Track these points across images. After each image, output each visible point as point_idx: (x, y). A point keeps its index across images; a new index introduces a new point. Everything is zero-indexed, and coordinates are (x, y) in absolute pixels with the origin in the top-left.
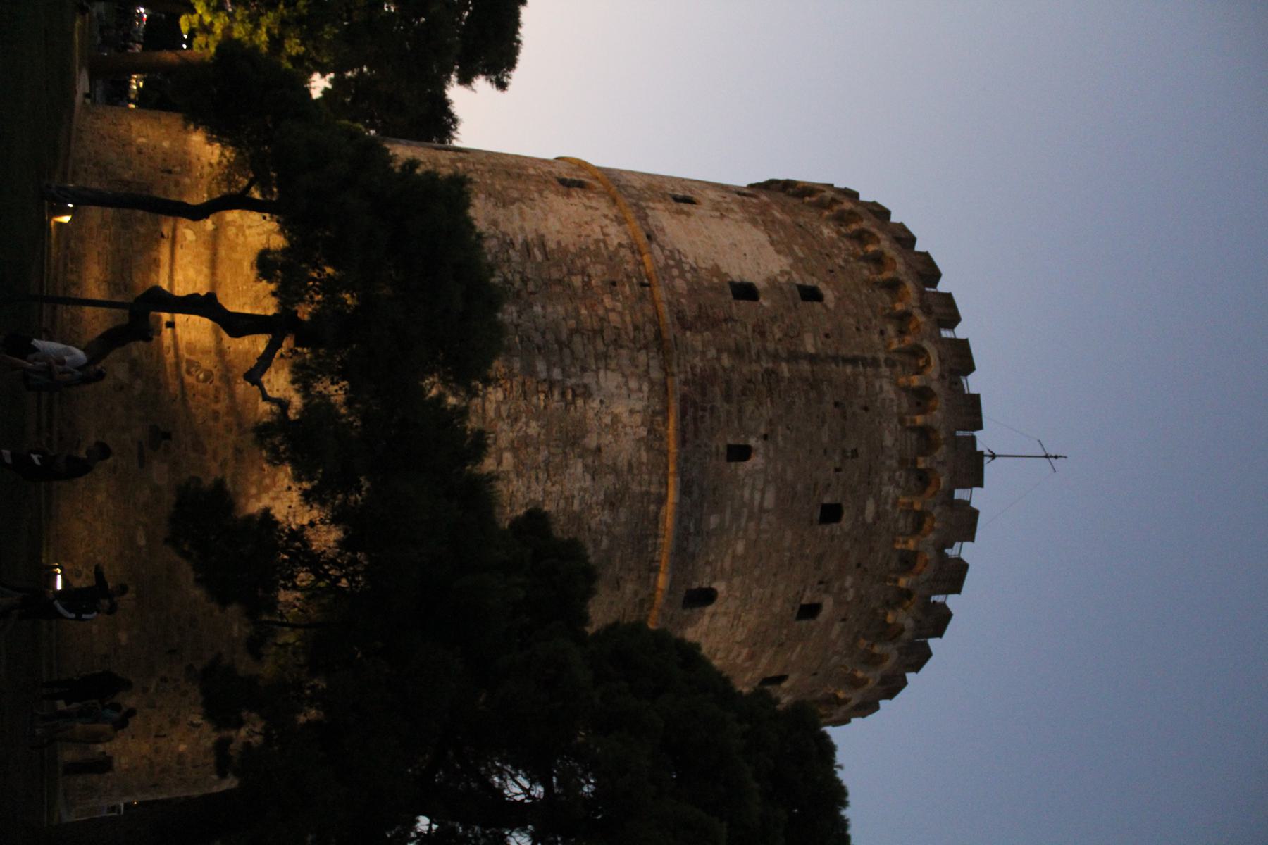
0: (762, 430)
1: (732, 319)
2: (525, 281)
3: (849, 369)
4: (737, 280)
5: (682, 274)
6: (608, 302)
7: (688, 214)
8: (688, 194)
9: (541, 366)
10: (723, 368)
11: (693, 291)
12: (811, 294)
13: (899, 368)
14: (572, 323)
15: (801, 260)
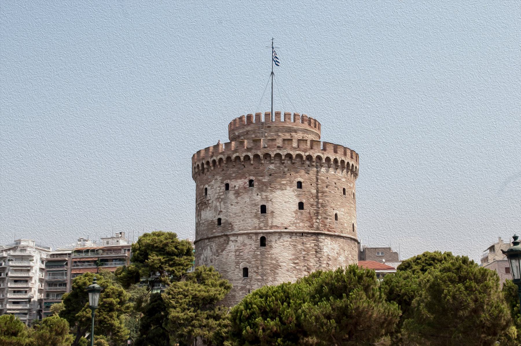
0: (332, 210)
1: (309, 213)
2: (305, 266)
3: (319, 181)
4: (298, 207)
5: (299, 223)
6: (308, 246)
7: (273, 212)
8: (259, 206)
9: (324, 265)
10: (321, 218)
11: (302, 221)
12: (300, 185)
13: (318, 164)
14: (314, 256)
15: (287, 184)
